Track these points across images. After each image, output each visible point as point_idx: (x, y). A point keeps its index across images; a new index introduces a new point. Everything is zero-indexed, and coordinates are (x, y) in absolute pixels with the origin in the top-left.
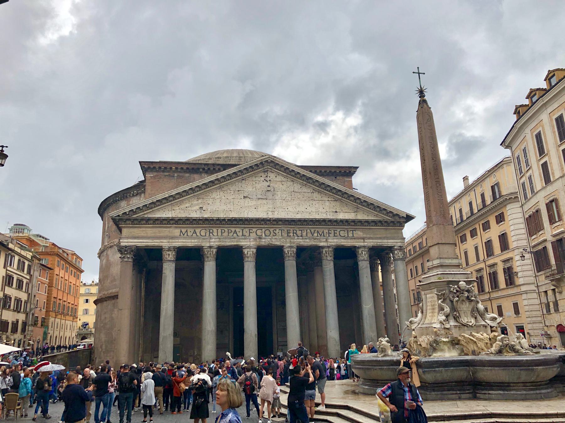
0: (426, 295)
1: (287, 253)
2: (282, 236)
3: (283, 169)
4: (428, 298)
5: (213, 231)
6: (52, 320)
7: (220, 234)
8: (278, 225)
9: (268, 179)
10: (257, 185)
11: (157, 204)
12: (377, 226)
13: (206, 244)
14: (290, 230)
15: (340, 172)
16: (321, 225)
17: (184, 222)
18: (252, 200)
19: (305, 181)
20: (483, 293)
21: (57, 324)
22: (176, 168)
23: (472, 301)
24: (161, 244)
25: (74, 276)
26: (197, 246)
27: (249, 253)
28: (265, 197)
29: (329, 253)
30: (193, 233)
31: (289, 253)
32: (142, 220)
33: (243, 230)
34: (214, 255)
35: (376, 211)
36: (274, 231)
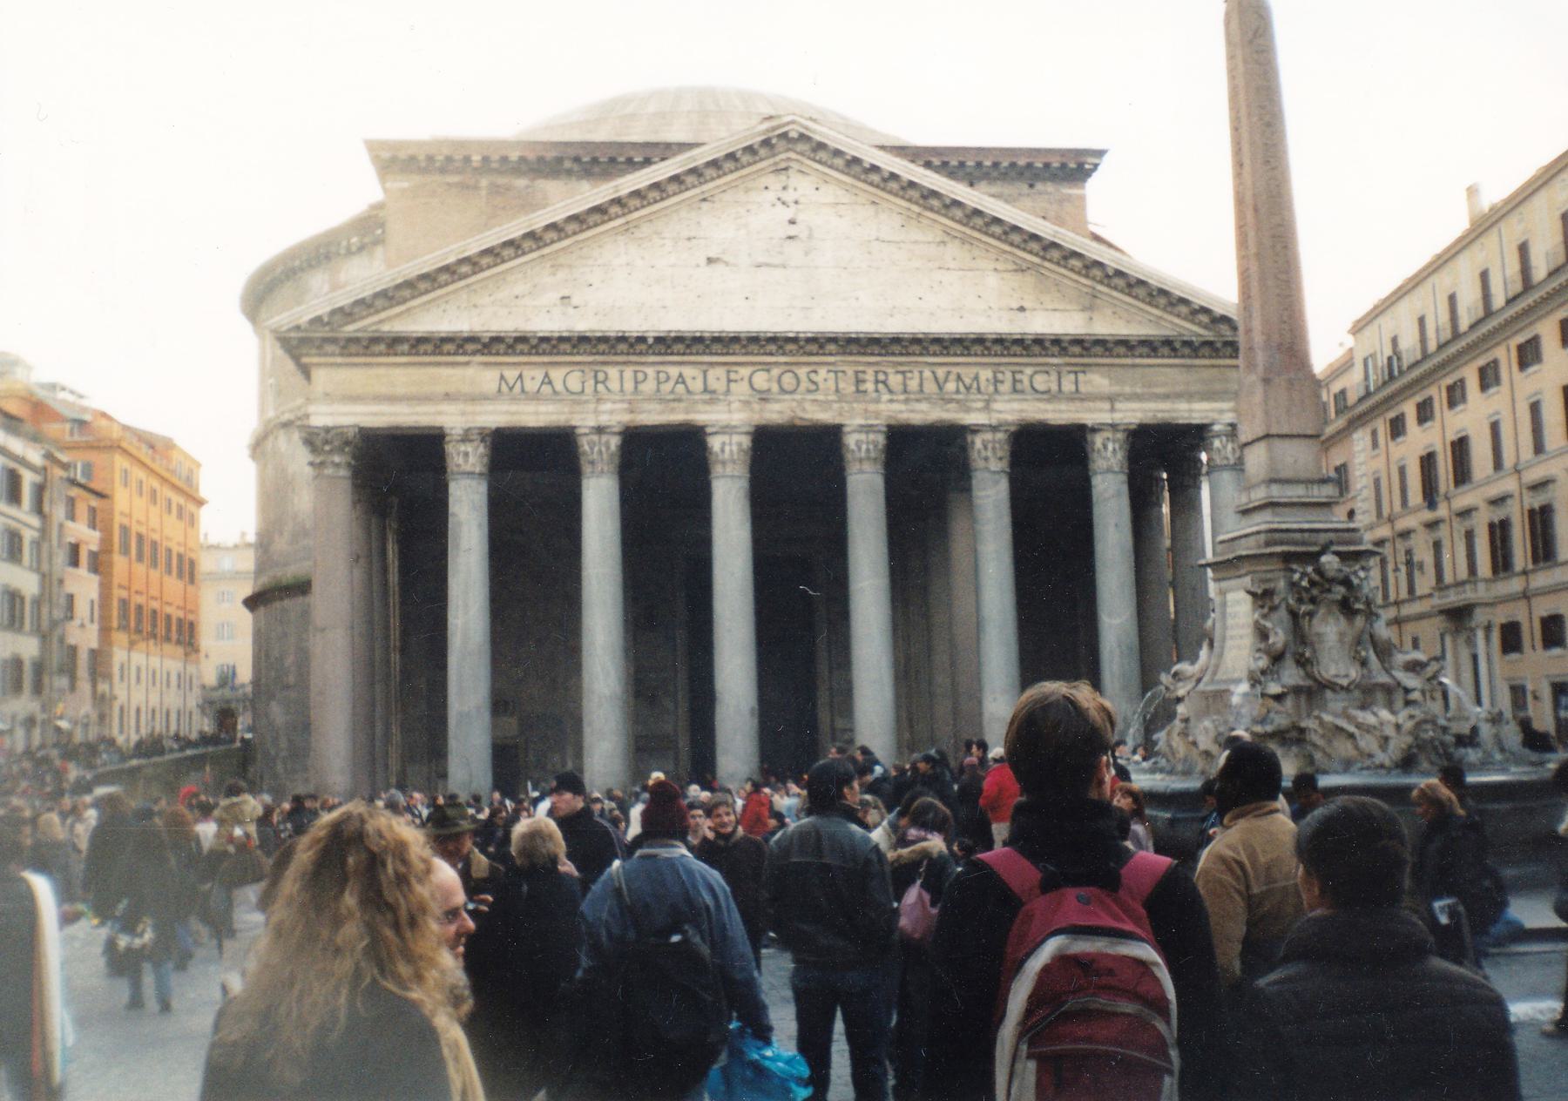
0: (1223, 593)
1: (853, 451)
2: (837, 390)
3: (839, 162)
4: (1229, 604)
5: (606, 373)
6: (119, 655)
7: (629, 386)
8: (824, 354)
9: (789, 196)
11: (422, 286)
13: (583, 419)
14: (864, 372)
15: (1047, 165)
16: (969, 355)
17: (510, 347)
19: (917, 203)
20: (1506, 575)
21: (139, 670)
22: (486, 159)
23: (1357, 612)
25: (180, 516)
27: (727, 448)
30: (543, 383)
32: (375, 340)
33: (705, 373)
34: (612, 455)
35: (1157, 307)
36: (813, 376)
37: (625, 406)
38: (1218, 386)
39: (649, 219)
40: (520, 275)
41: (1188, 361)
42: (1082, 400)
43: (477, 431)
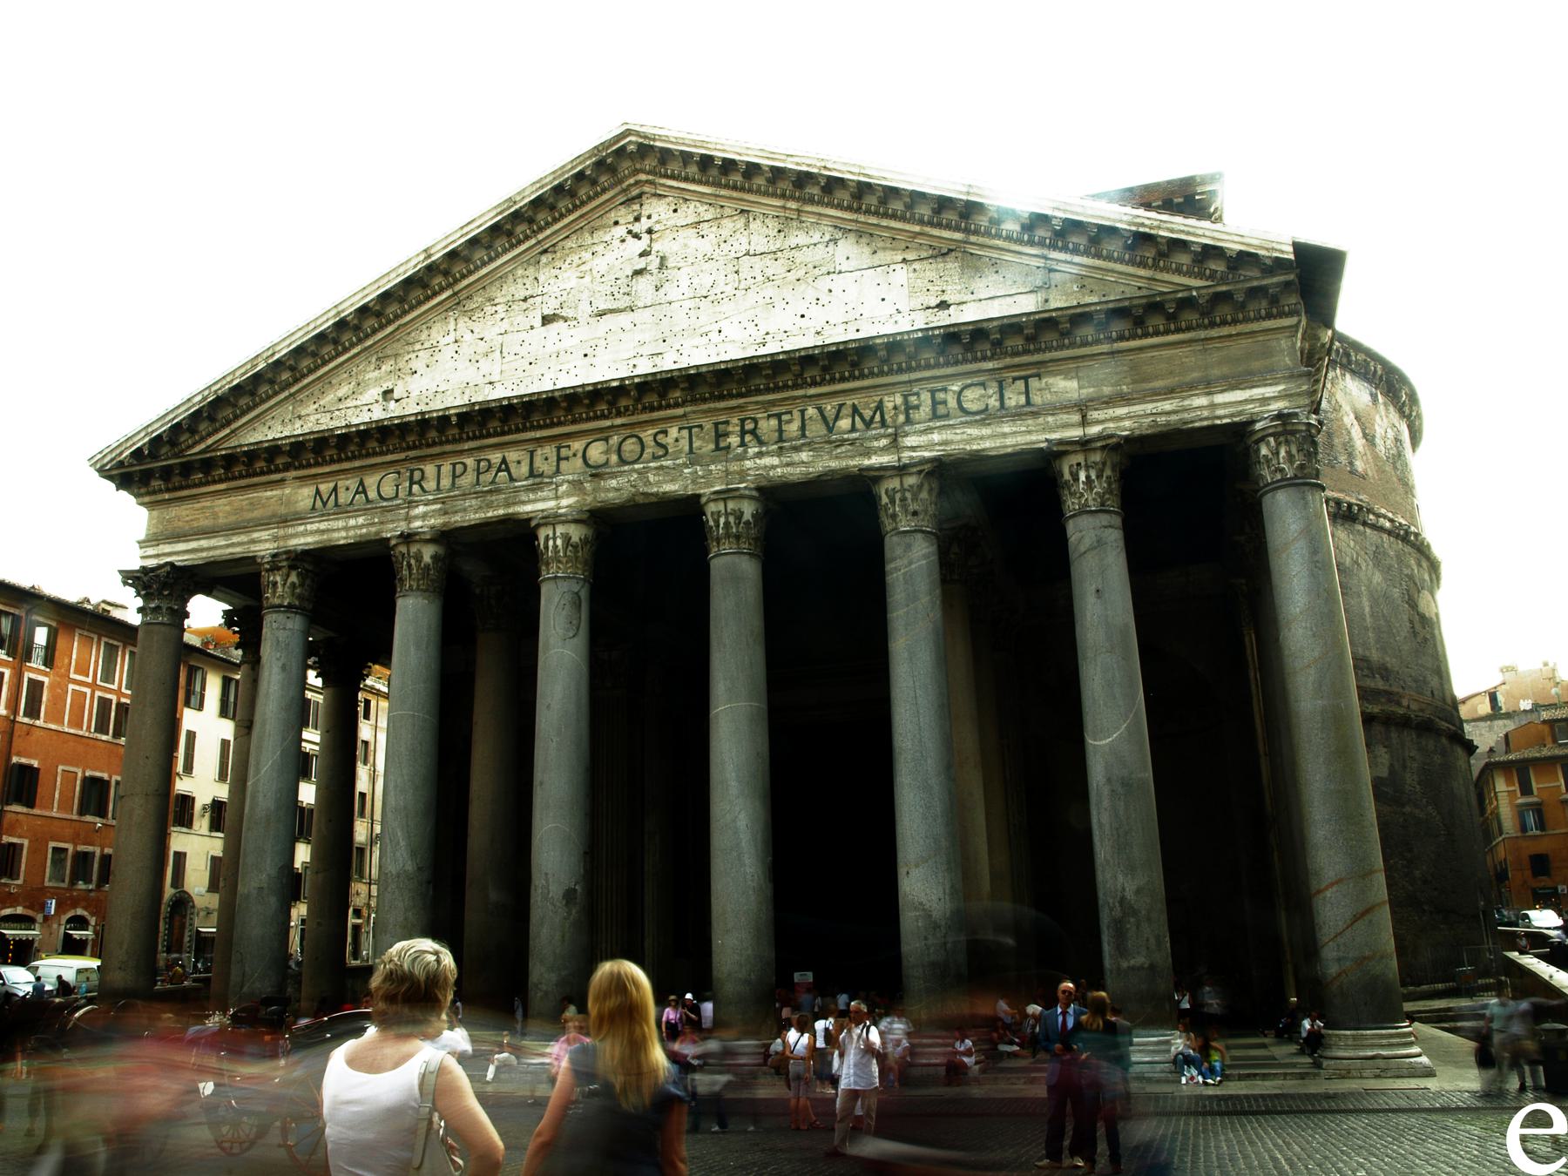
5: (422, 471)
7: (446, 482)
8: (669, 406)
9: (645, 224)
10: (598, 260)
11: (244, 401)
12: (1146, 335)
13: (391, 530)
14: (727, 423)
18: (575, 323)
19: (792, 198)
24: (253, 548)
26: (369, 542)
27: (551, 543)
28: (623, 302)
29: (903, 499)
30: (357, 492)
31: (718, 526)
32: (187, 469)
34: (427, 567)
36: (660, 437)
37: (438, 506)
38: (1256, 365)
39: (483, 285)
40: (345, 375)
41: (1202, 334)
42: (1035, 414)
43: (284, 557)
